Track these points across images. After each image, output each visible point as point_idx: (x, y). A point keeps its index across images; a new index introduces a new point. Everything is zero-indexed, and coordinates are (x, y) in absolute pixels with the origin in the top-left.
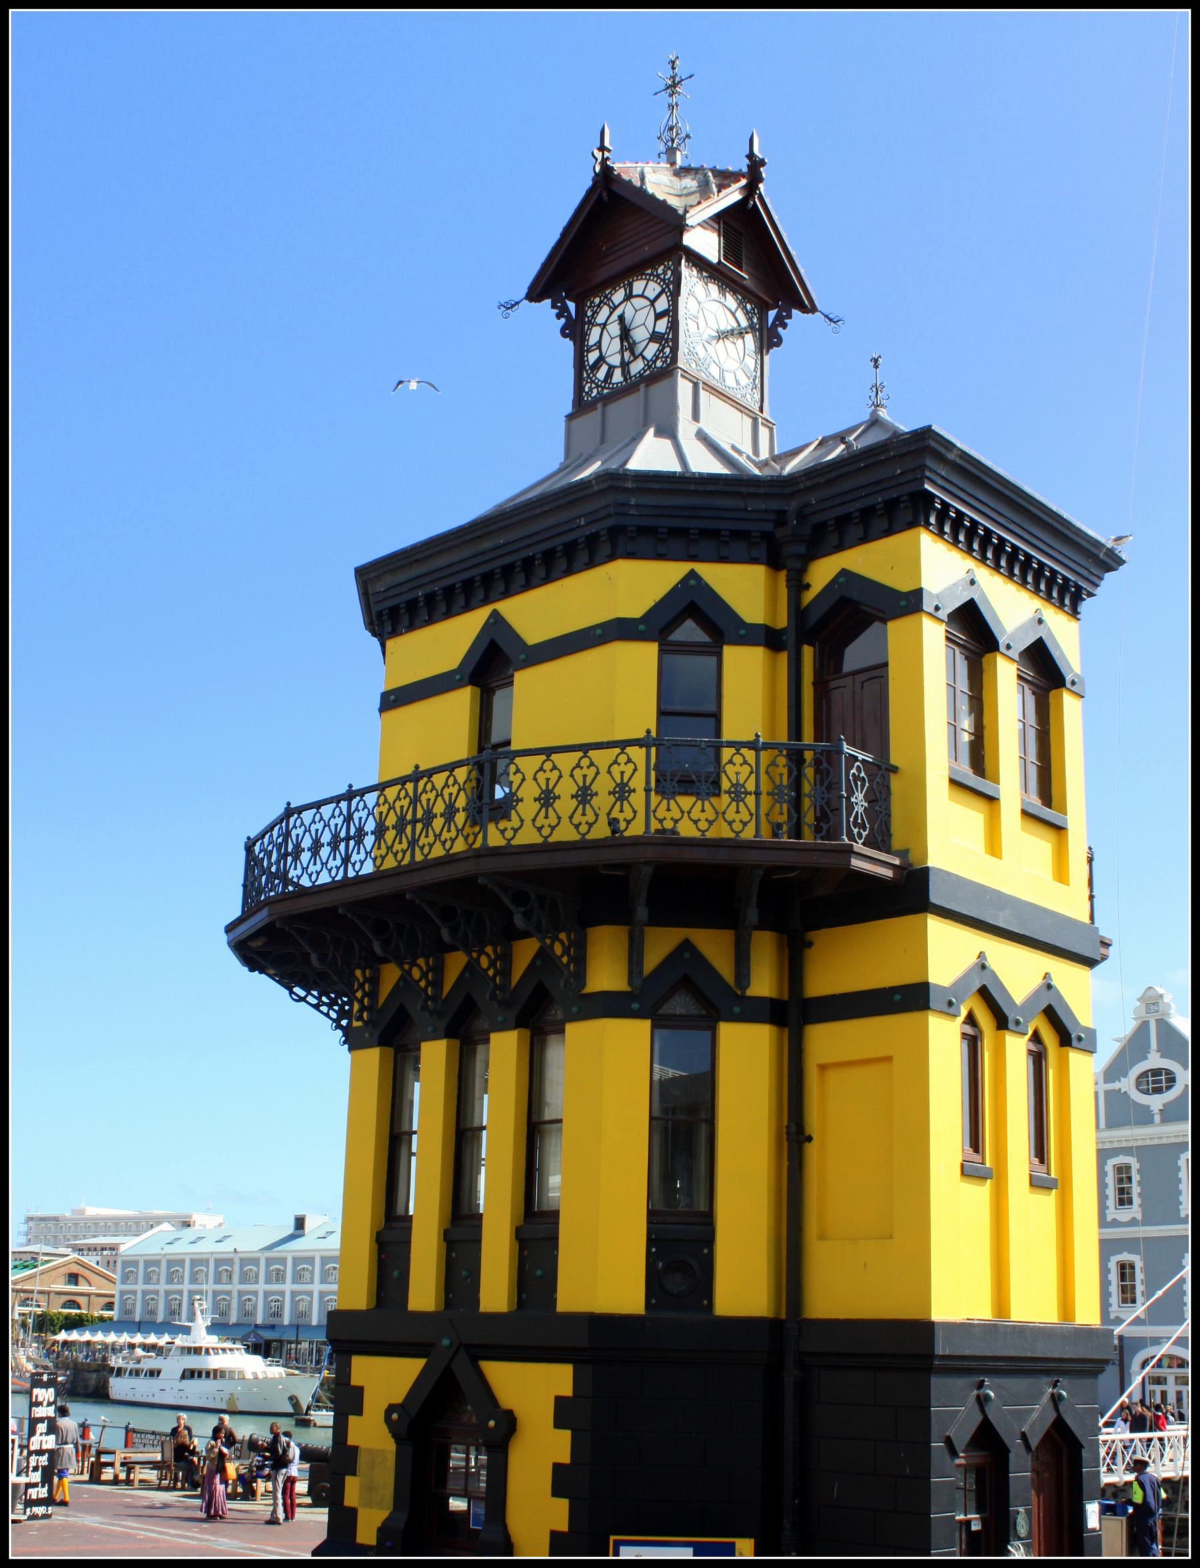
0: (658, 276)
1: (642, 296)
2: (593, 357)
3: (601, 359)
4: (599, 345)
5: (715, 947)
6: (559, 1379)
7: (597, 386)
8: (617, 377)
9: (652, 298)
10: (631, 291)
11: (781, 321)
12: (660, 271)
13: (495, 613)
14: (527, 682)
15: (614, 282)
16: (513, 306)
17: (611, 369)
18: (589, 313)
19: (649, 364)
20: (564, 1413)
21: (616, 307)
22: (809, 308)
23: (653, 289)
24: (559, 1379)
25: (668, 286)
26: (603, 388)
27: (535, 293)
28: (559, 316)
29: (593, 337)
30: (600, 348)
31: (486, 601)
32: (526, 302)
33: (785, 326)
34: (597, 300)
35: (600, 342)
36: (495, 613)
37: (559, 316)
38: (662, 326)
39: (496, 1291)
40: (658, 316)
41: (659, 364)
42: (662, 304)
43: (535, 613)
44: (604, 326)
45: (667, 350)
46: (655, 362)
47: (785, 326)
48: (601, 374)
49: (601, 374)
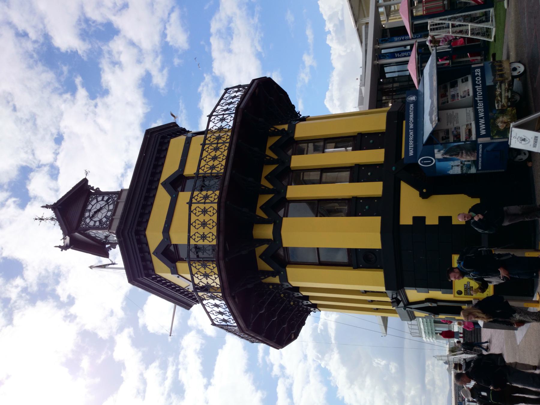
1: (93, 206)
2: (97, 224)
3: (100, 221)
4: (95, 222)
12: (90, 200)
23: (95, 201)
31: (157, 188)
34: (83, 223)
39: (376, 156)
43: (169, 169)
48: (104, 220)
49: (104, 220)
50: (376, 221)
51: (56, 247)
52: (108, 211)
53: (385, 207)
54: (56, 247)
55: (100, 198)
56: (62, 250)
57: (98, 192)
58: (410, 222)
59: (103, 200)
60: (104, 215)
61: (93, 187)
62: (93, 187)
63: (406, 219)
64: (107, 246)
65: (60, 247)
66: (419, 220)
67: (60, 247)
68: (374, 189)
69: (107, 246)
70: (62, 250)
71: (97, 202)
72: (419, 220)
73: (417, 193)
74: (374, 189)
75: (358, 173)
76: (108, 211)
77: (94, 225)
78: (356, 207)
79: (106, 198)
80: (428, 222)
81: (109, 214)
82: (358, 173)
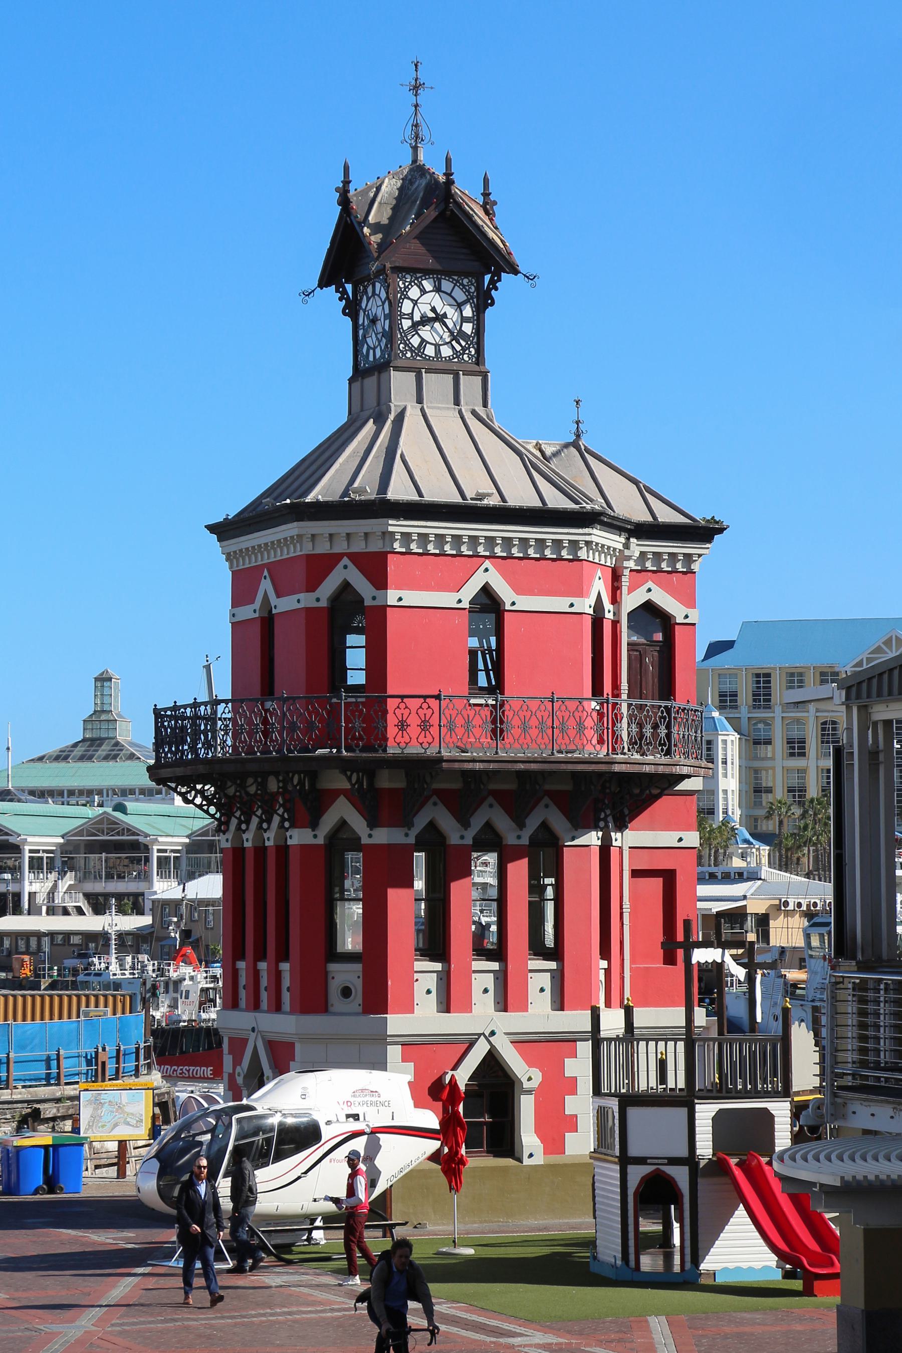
0: (462, 284)
1: (450, 295)
4: (411, 316)
7: (412, 351)
8: (430, 351)
9: (459, 301)
10: (440, 284)
12: (465, 281)
21: (423, 292)
23: (460, 295)
25: (472, 298)
26: (417, 355)
30: (412, 318)
35: (412, 313)
38: (468, 328)
44: (415, 302)
45: (473, 351)
49: (415, 341)
51: (346, 169)
54: (346, 169)
55: (468, 311)
56: (337, 190)
57: (483, 301)
59: (464, 320)
61: (496, 289)
62: (496, 289)
64: (349, 287)
65: (347, 182)
67: (347, 182)
69: (349, 287)
70: (337, 190)
76: (437, 346)
77: (402, 316)
79: (468, 328)
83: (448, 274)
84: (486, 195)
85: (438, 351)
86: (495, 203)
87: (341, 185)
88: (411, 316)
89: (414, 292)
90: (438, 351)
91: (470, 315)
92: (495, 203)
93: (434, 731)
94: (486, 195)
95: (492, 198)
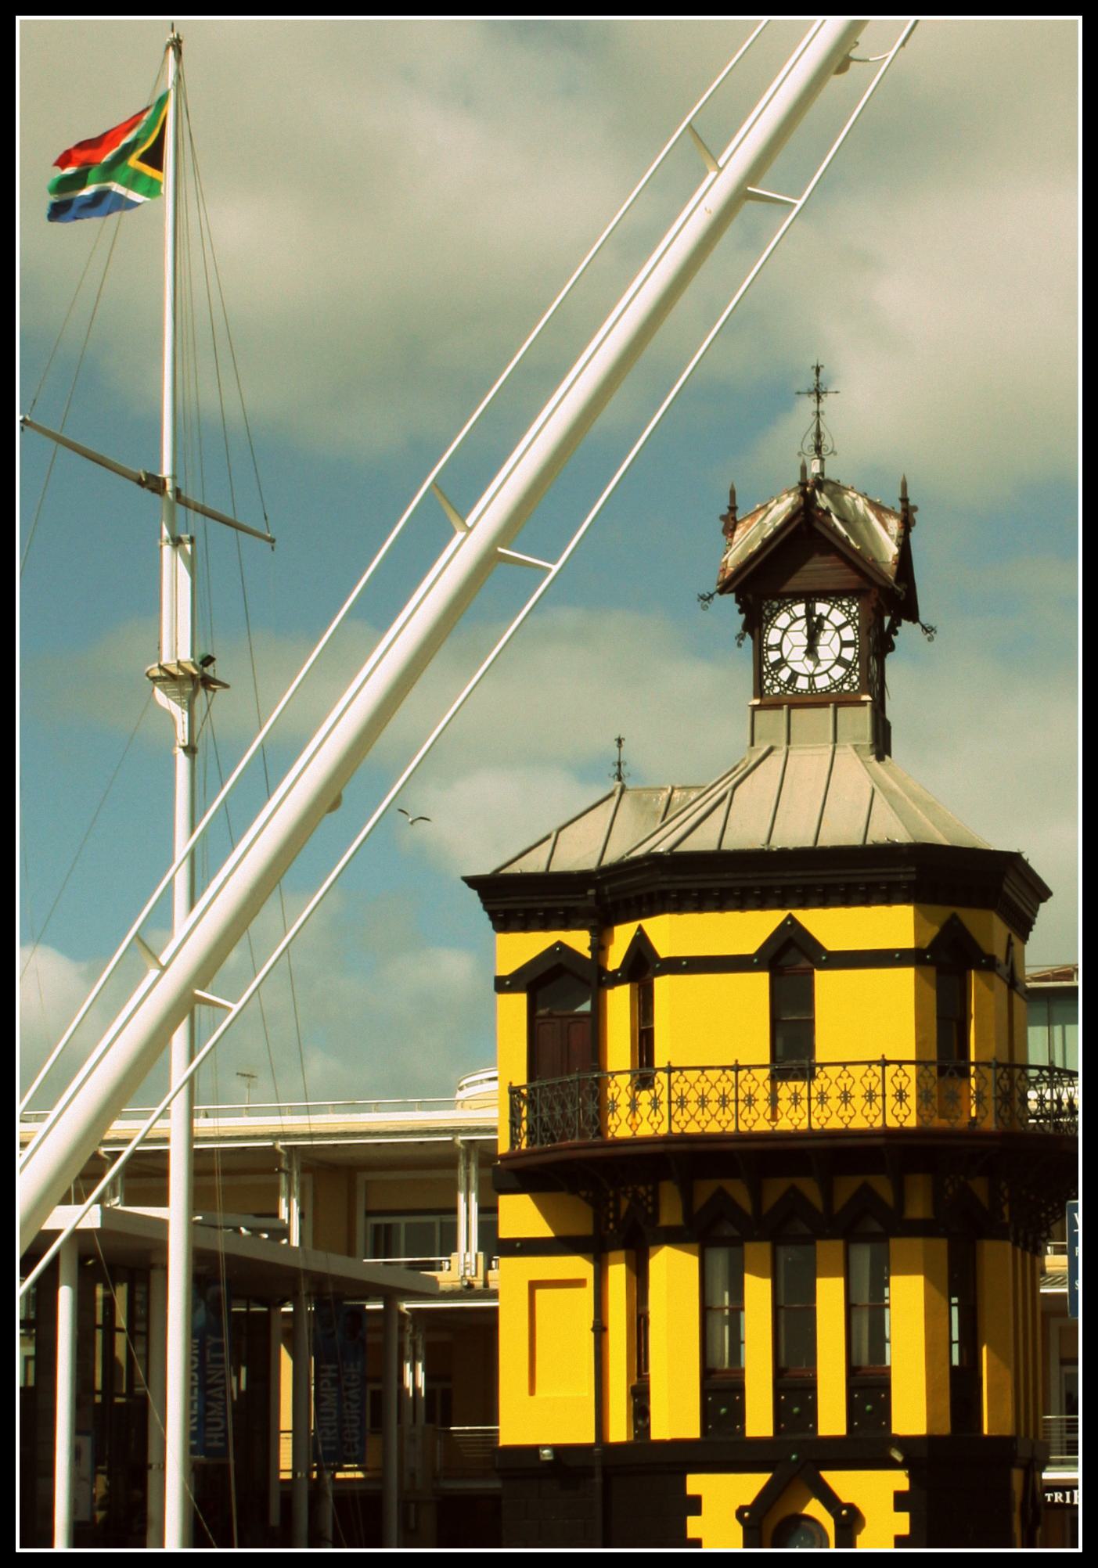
0: (843, 607)
2: (773, 656)
3: (781, 663)
4: (779, 647)
5: (979, 1187)
6: (900, 1480)
7: (779, 685)
8: (802, 683)
9: (838, 624)
11: (893, 630)
13: (790, 917)
14: (825, 981)
15: (796, 597)
16: (708, 599)
17: (794, 676)
18: (767, 613)
19: (836, 684)
20: (901, 1501)
22: (914, 617)
23: (838, 617)
24: (900, 1480)
27: (721, 591)
28: (741, 612)
29: (773, 637)
31: (781, 906)
32: (717, 596)
33: (896, 633)
36: (790, 917)
37: (741, 612)
40: (845, 644)
41: (846, 687)
42: (849, 634)
43: (833, 926)
44: (785, 631)
45: (855, 678)
46: (844, 681)
47: (896, 633)
48: (784, 674)
49: (784, 674)
50: (691, 1430)
51: (733, 494)
52: (811, 676)
53: (721, 1445)
54: (733, 494)
55: (849, 634)
56: (723, 518)
58: (691, 1489)
59: (845, 644)
60: (798, 667)
63: (696, 1483)
65: (733, 509)
66: (695, 1505)
67: (733, 509)
68: (759, 1421)
70: (723, 518)
71: (838, 629)
72: (695, 1505)
73: (748, 1501)
74: (759, 1421)
75: (795, 1389)
77: (770, 648)
78: (721, 1390)
79: (849, 654)
80: (691, 1520)
81: (802, 683)
82: (795, 1389)
83: (825, 596)
84: (904, 500)
85: (812, 684)
86: (915, 509)
87: (726, 511)
88: (779, 647)
89: (783, 620)
90: (812, 684)
91: (852, 638)
92: (915, 509)
93: (664, 1108)
94: (904, 500)
95: (911, 503)
